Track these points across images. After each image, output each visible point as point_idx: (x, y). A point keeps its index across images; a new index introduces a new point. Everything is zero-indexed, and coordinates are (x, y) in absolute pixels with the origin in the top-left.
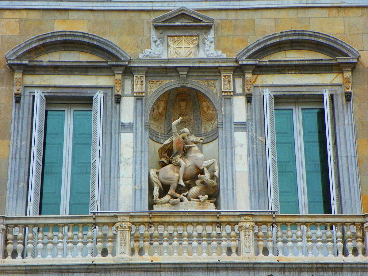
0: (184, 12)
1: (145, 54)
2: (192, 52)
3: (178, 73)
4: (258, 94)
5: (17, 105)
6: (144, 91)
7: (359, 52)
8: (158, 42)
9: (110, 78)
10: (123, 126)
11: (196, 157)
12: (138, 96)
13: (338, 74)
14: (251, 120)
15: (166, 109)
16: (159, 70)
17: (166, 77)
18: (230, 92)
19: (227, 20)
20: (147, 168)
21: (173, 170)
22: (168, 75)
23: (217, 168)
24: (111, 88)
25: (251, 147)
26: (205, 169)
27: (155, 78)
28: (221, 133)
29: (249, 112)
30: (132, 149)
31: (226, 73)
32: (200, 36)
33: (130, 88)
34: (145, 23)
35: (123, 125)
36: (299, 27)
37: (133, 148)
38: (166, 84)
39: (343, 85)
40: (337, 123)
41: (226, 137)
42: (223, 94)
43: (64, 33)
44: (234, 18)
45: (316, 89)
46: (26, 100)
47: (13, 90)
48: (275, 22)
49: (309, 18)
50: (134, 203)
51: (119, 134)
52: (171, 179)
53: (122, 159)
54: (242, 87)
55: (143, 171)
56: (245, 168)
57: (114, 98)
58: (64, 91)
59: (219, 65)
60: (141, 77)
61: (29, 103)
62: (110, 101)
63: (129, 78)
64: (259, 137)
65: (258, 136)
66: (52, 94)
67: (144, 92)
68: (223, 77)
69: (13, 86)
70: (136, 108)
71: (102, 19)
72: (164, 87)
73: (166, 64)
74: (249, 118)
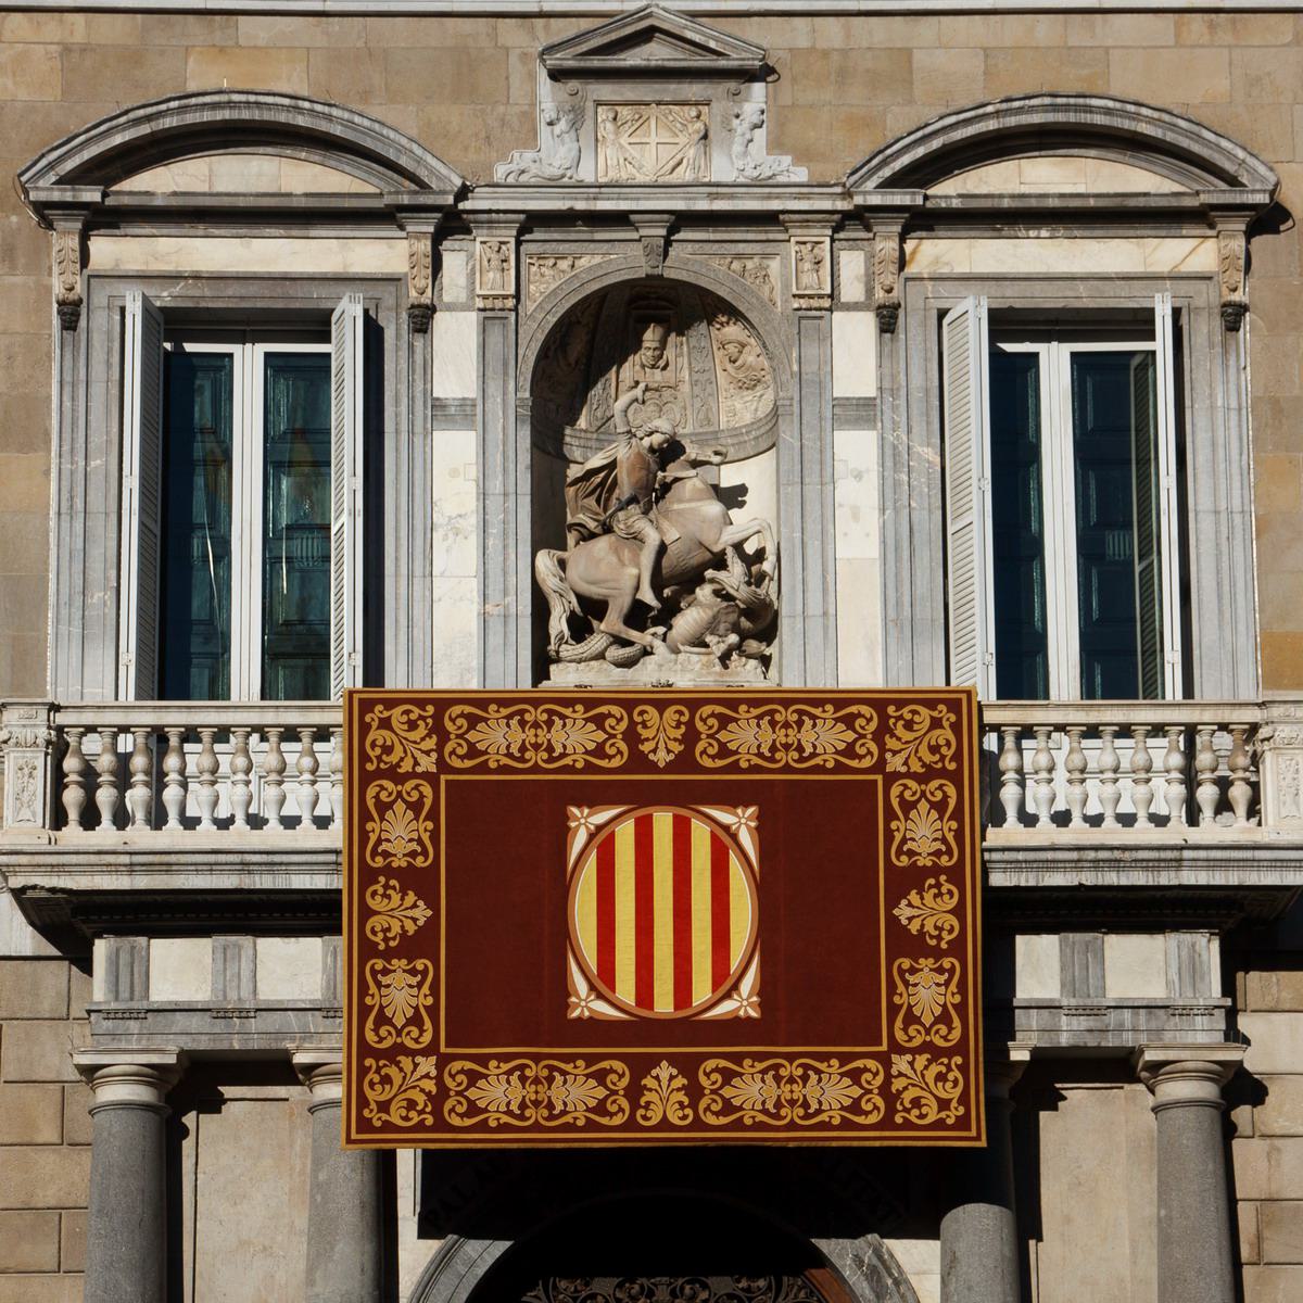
1: (514, 167)
2: (685, 161)
4: (921, 304)
5: (68, 335)
7: (1275, 166)
8: (562, 125)
10: (439, 410)
13: (1195, 242)
14: (894, 392)
17: (592, 245)
18: (821, 297)
19: (812, 50)
20: (529, 550)
21: (616, 551)
24: (393, 280)
25: (889, 482)
26: (730, 552)
27: (547, 246)
29: (886, 363)
31: (805, 231)
32: (713, 104)
33: (462, 281)
35: (438, 405)
36: (1070, 80)
39: (1216, 278)
40: (1188, 403)
43: (224, 98)
44: (838, 43)
45: (1123, 289)
46: (98, 322)
47: (49, 289)
48: (985, 62)
49: (1107, 49)
52: (609, 585)
54: (864, 279)
56: (873, 550)
57: (404, 316)
58: (230, 292)
59: (781, 208)
60: (502, 243)
61: (109, 332)
63: (457, 247)
64: (920, 449)
66: (190, 304)
69: (50, 275)
70: (483, 346)
71: (360, 44)
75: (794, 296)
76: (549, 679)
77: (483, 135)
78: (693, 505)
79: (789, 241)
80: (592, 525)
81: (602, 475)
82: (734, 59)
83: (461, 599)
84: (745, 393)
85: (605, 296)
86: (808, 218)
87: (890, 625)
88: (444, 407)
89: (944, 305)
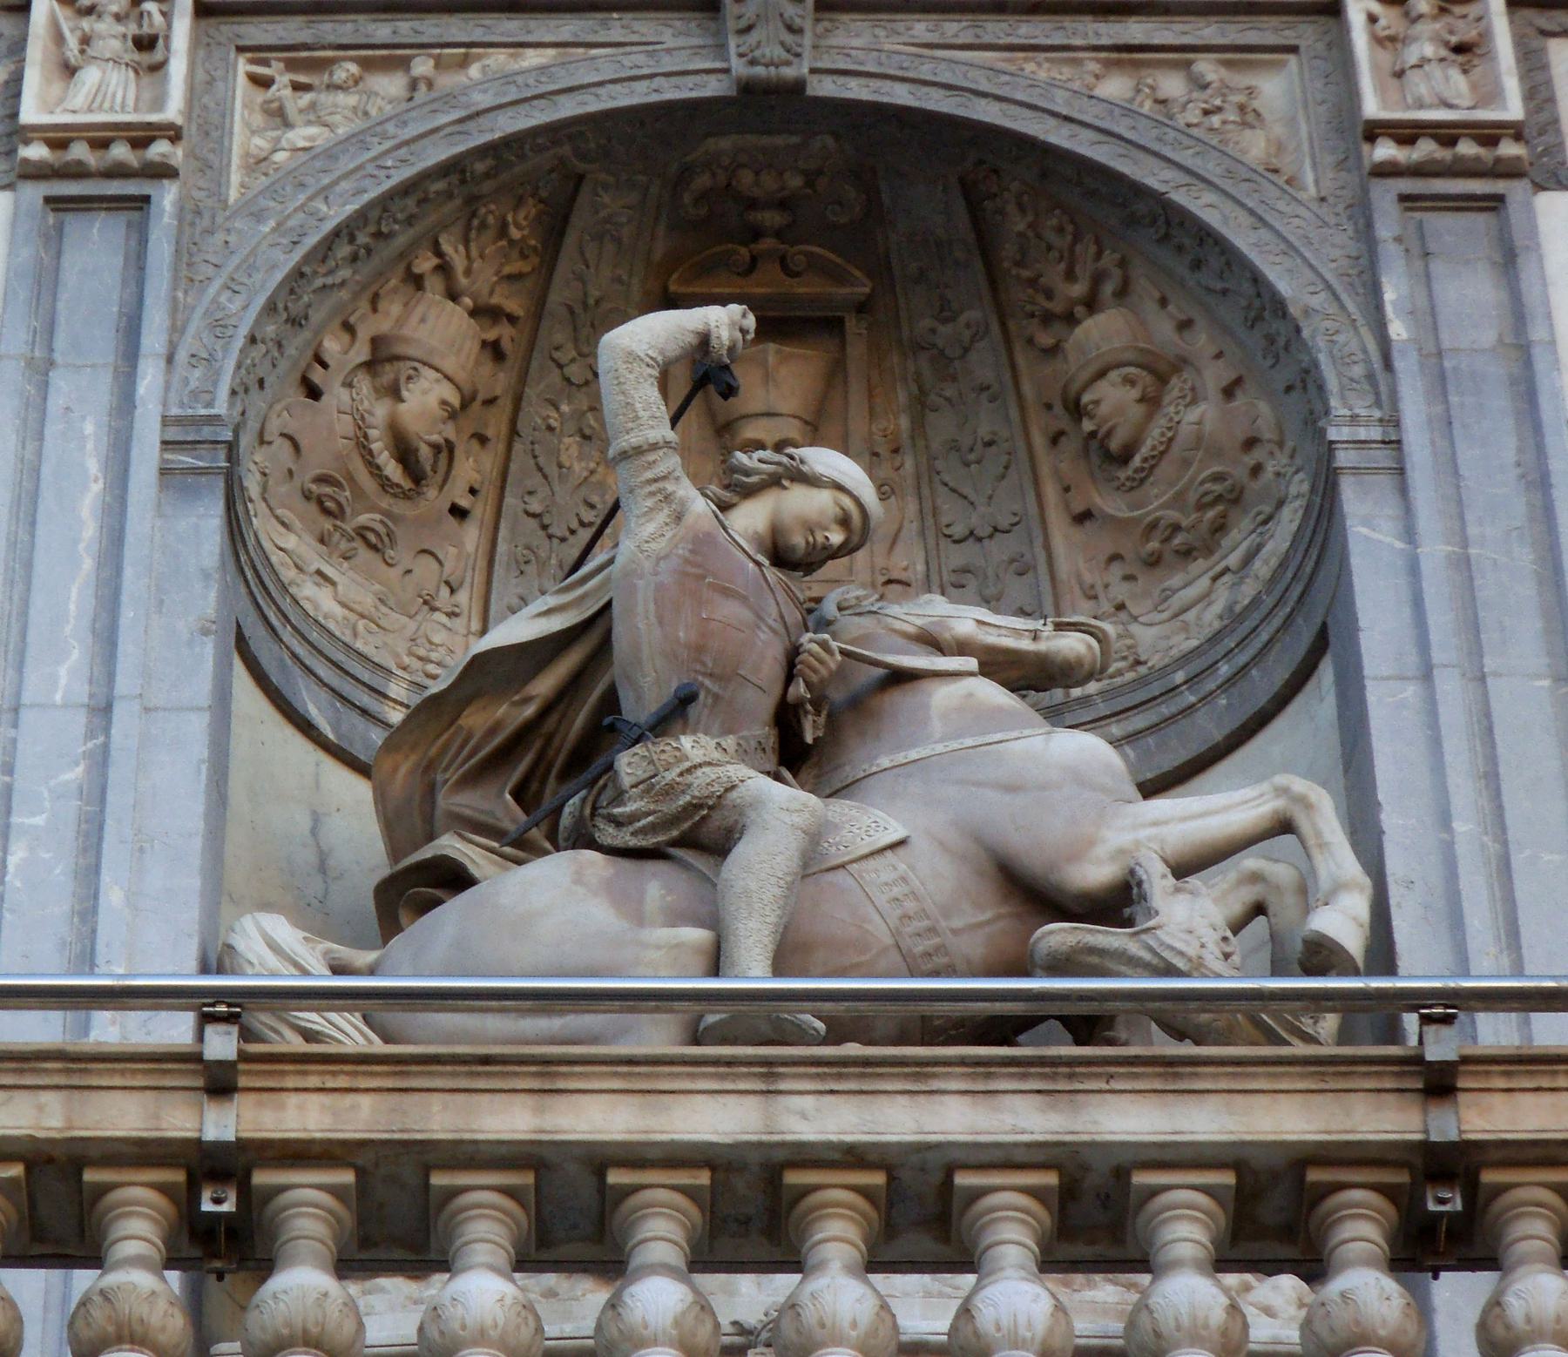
6: (173, 111)
12: (77, 172)
15: (514, 432)
18: (1489, 134)
26: (1158, 881)
38: (508, 78)
41: (1463, 564)
42: (1385, 151)
55: (113, 896)
67: (174, 133)
72: (482, 100)
75: (1374, 130)
81: (545, 685)
84: (1176, 580)
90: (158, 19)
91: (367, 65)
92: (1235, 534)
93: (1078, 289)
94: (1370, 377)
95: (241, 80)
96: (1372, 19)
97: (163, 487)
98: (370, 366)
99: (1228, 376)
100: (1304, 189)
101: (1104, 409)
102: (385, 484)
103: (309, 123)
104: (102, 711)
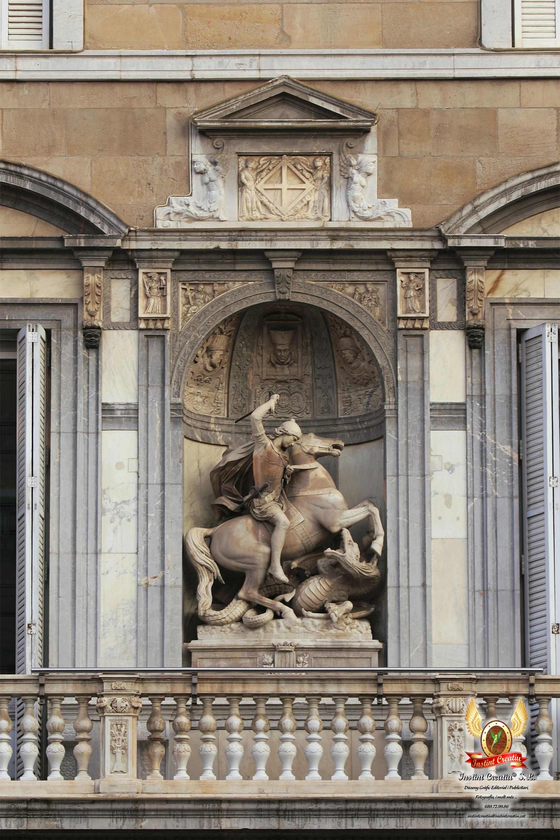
0: (288, 91)
3: (270, 263)
6: (168, 315)
9: (68, 277)
11: (320, 499)
12: (151, 329)
14: (482, 398)
16: (213, 257)
17: (233, 274)
18: (422, 319)
19: (415, 110)
22: (238, 267)
23: (379, 529)
25: (477, 475)
26: (347, 535)
28: (394, 432)
29: (476, 375)
30: (136, 474)
32: (335, 157)
33: (127, 304)
34: (170, 119)
35: (108, 409)
37: (138, 473)
41: (407, 443)
42: (401, 325)
44: (436, 104)
50: (142, 624)
51: (97, 433)
53: (106, 504)
54: (456, 303)
57: (80, 334)
62: (71, 344)
65: (498, 443)
67: (168, 318)
68: (400, 278)
70: (144, 362)
71: (45, 106)
73: (234, 243)
74: (476, 392)
75: (400, 318)
76: (196, 638)
77: (144, 182)
78: (315, 492)
79: (395, 270)
80: (232, 506)
81: (240, 465)
82: (350, 121)
83: (125, 572)
84: (359, 388)
85: (245, 312)
86: (410, 255)
87: (477, 594)
88: (112, 411)
89: (524, 326)
90: (164, 282)
91: (204, 284)
92: (369, 386)
93: (342, 332)
94: (394, 387)
95: (181, 290)
96: (402, 281)
97: (171, 421)
98: (207, 351)
99: (370, 359)
100: (385, 325)
101: (346, 355)
102: (209, 372)
103: (194, 305)
104: (163, 484)
